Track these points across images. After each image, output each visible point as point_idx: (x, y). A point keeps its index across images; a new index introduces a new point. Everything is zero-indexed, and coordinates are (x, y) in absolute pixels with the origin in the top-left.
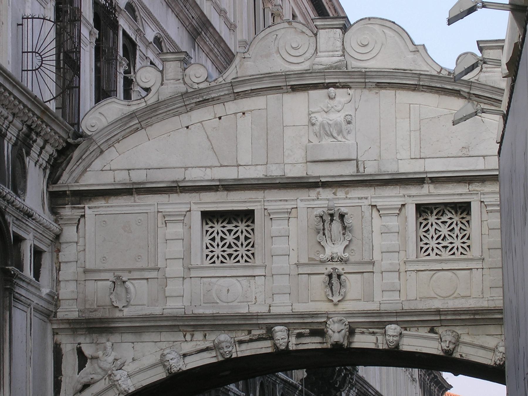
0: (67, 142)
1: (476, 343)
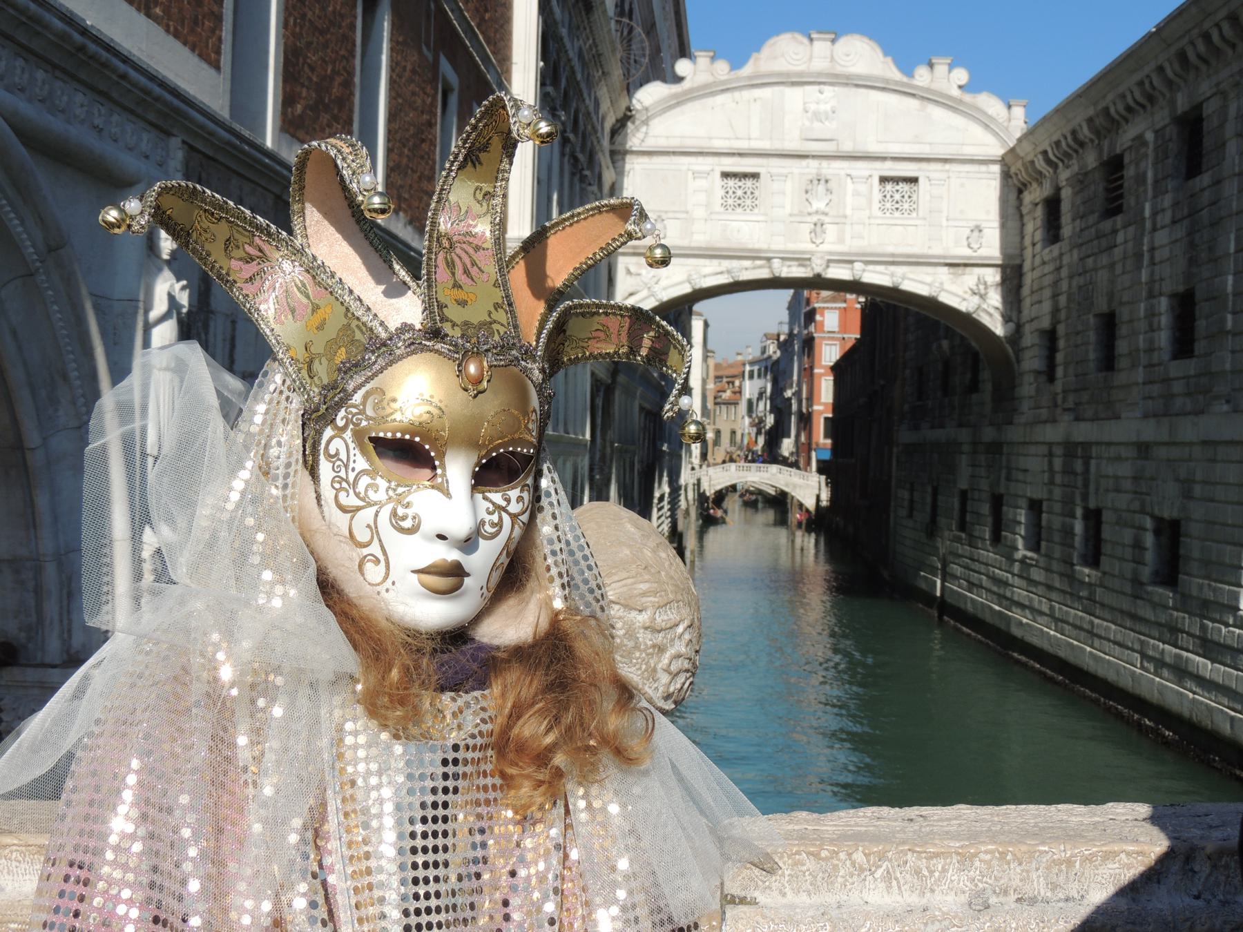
1: (916, 278)
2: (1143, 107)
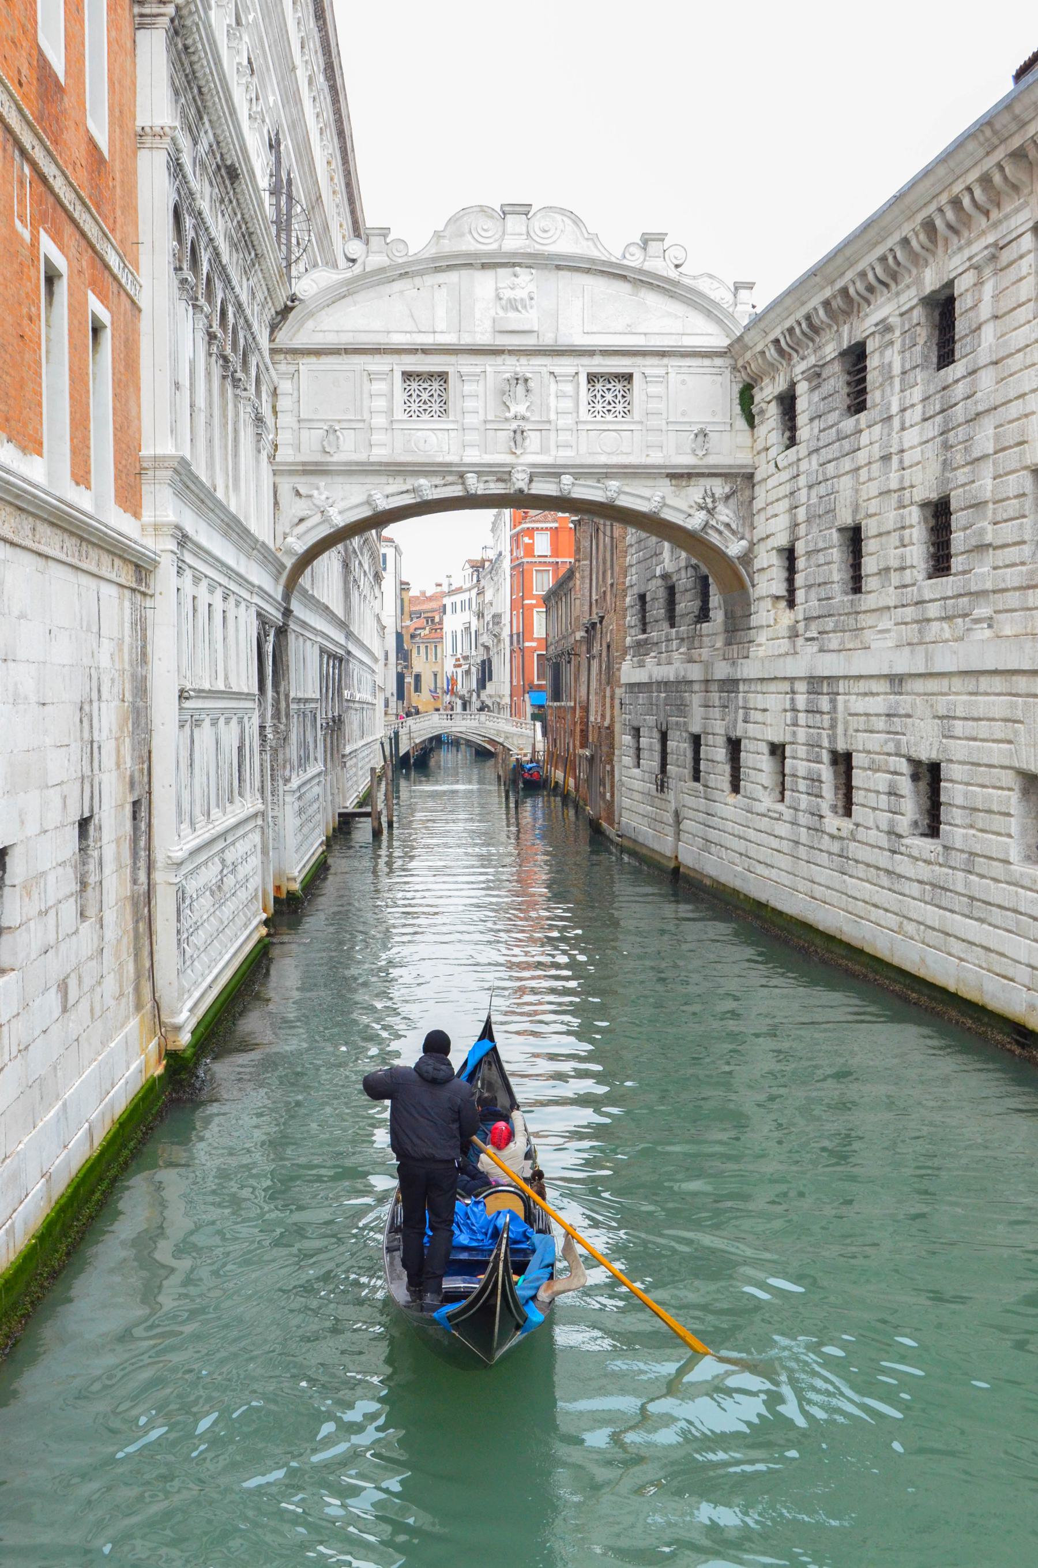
0: (286, 306)
2: (886, 285)
